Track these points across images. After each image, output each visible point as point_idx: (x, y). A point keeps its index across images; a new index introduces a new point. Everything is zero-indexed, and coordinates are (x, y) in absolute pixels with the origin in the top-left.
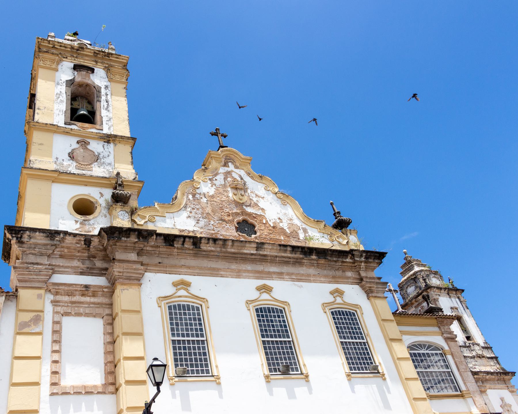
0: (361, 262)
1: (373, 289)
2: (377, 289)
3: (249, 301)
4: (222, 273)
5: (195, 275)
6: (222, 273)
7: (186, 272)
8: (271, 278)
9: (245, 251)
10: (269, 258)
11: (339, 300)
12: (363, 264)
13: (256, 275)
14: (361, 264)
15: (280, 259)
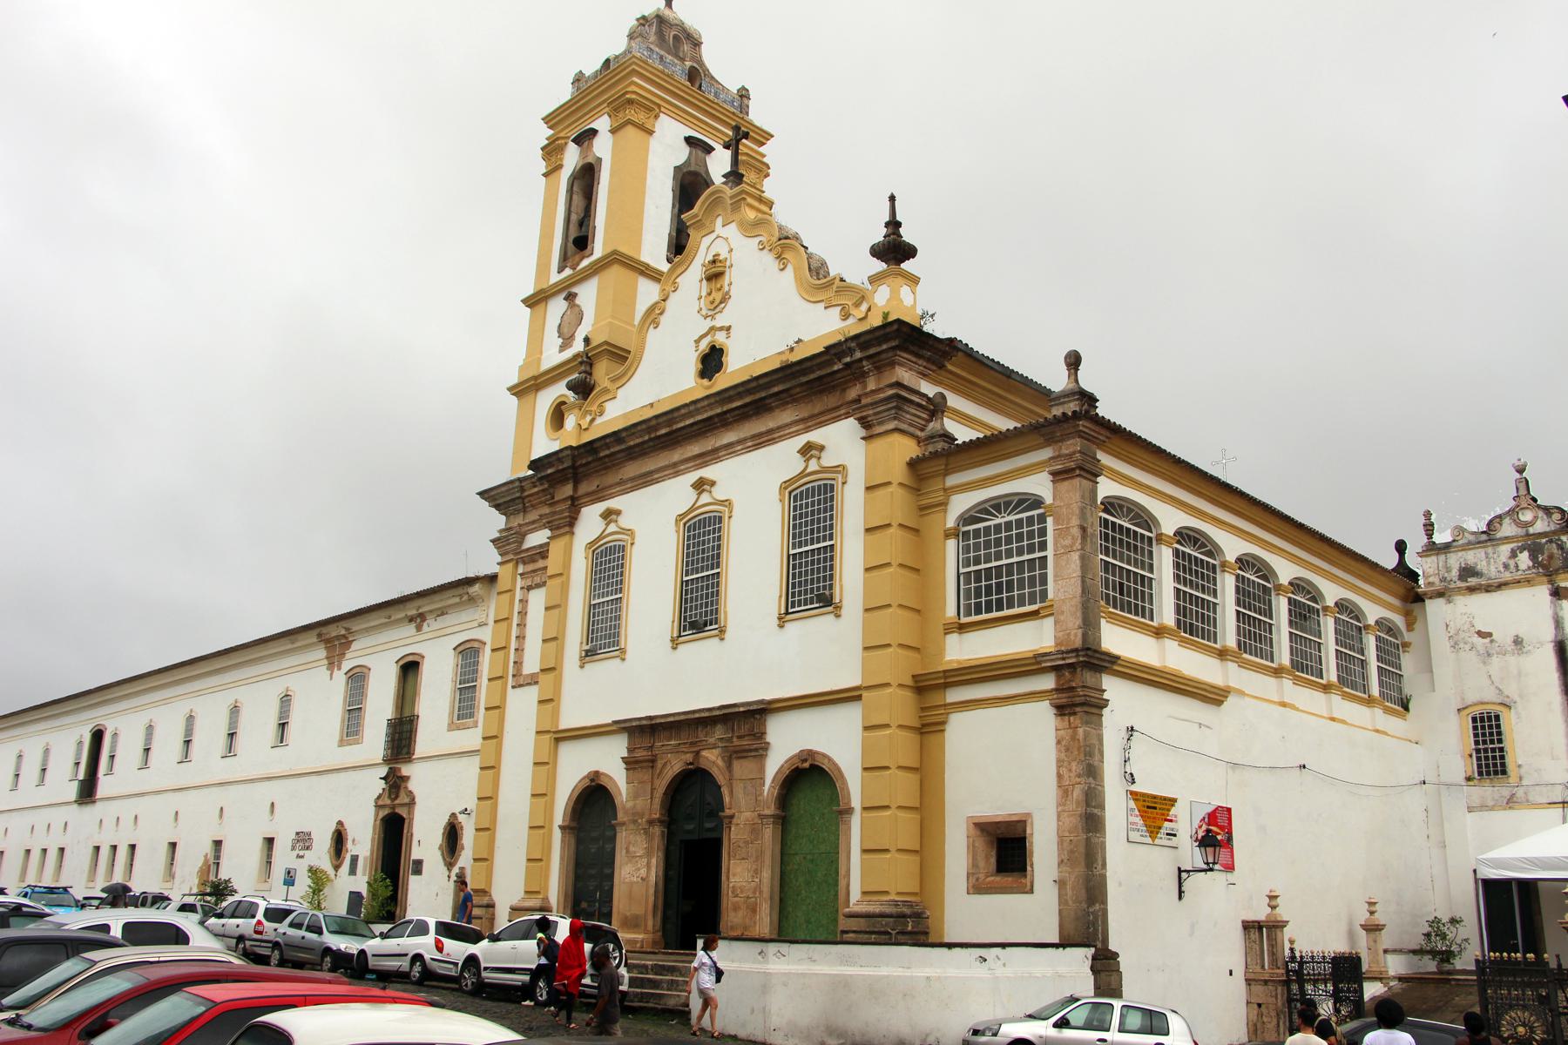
0: (860, 360)
1: (869, 419)
2: (877, 417)
3: (680, 515)
4: (656, 476)
5: (628, 492)
6: (656, 476)
7: (618, 491)
8: (718, 459)
9: (681, 425)
10: (716, 420)
11: (813, 466)
12: (865, 363)
13: (697, 462)
14: (860, 365)
15: (732, 414)
